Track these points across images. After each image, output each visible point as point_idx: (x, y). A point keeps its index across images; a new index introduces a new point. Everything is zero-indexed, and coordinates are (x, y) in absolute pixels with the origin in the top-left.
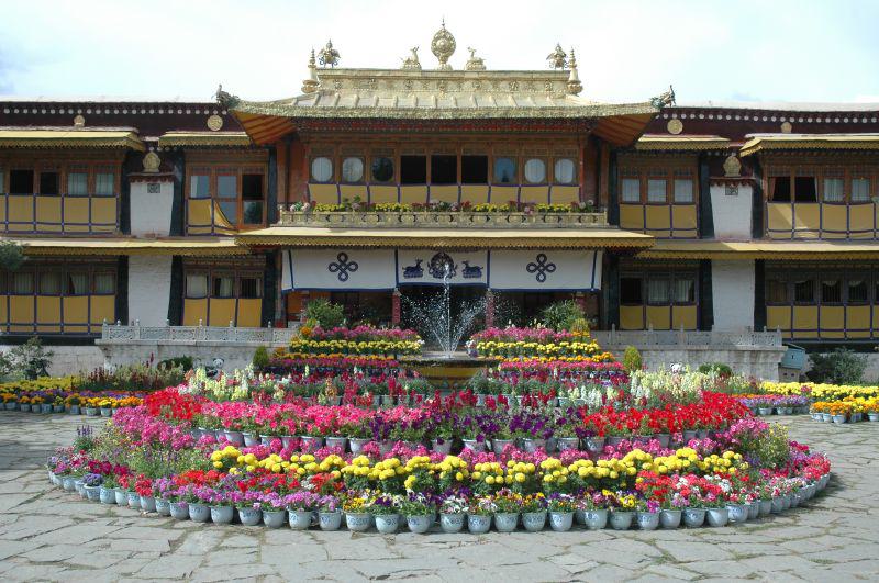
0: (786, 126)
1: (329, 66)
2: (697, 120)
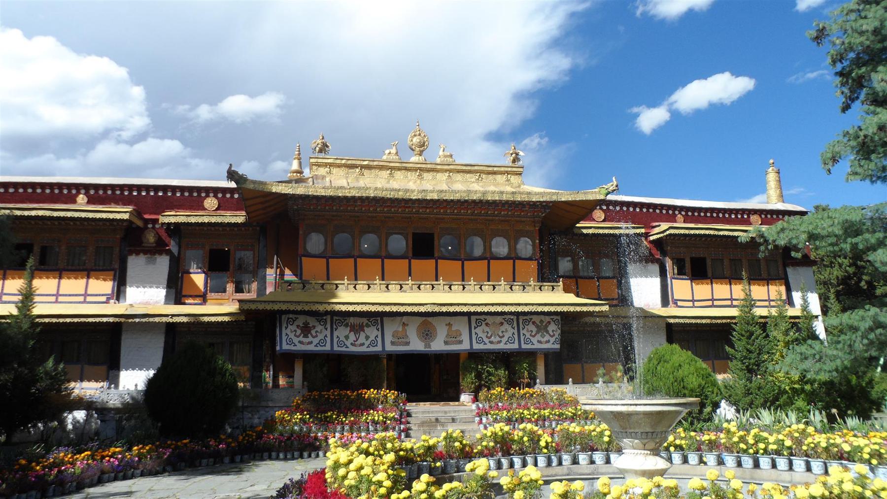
0: (680, 217)
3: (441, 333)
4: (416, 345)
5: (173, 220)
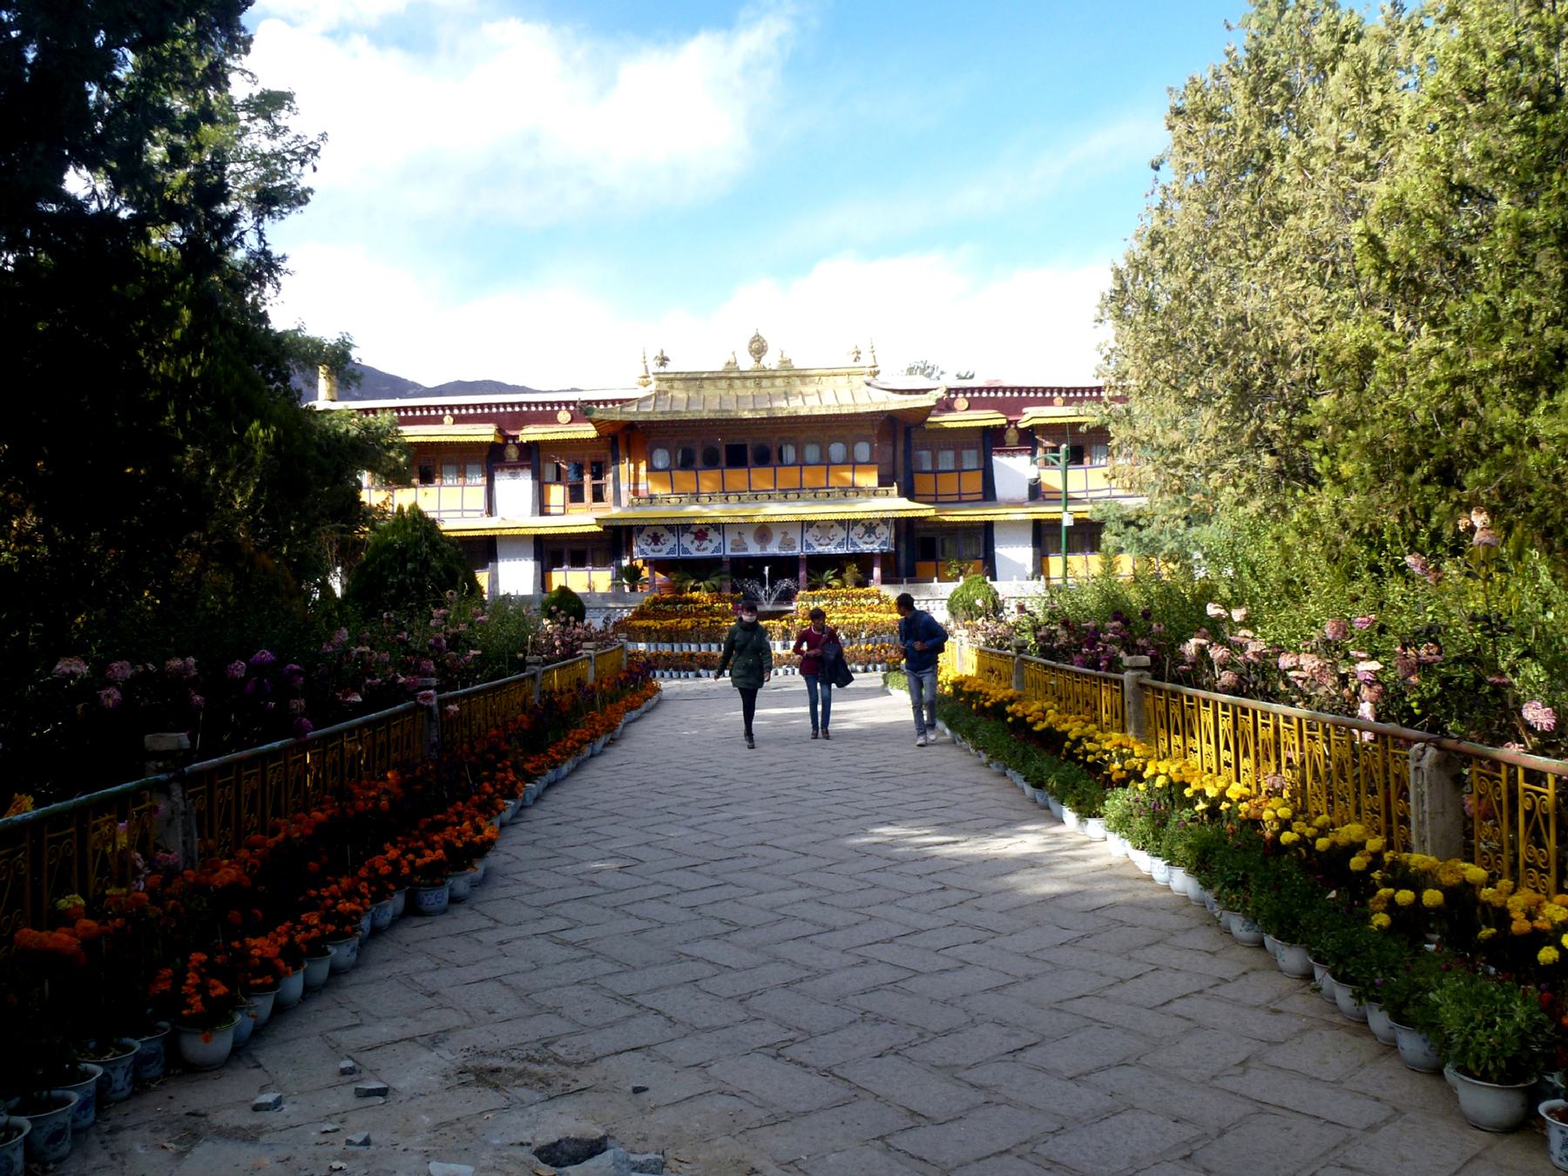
1: (662, 369)
2: (980, 397)
3: (777, 538)
4: (754, 550)
5: (532, 438)
